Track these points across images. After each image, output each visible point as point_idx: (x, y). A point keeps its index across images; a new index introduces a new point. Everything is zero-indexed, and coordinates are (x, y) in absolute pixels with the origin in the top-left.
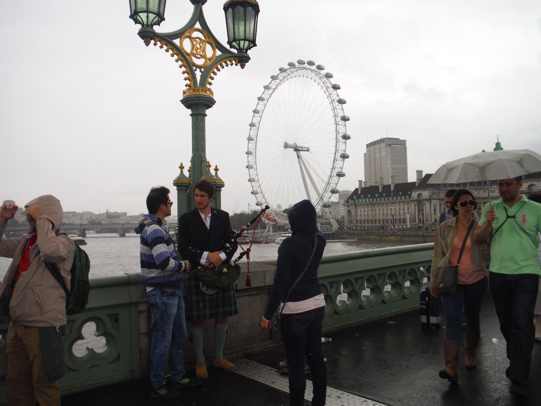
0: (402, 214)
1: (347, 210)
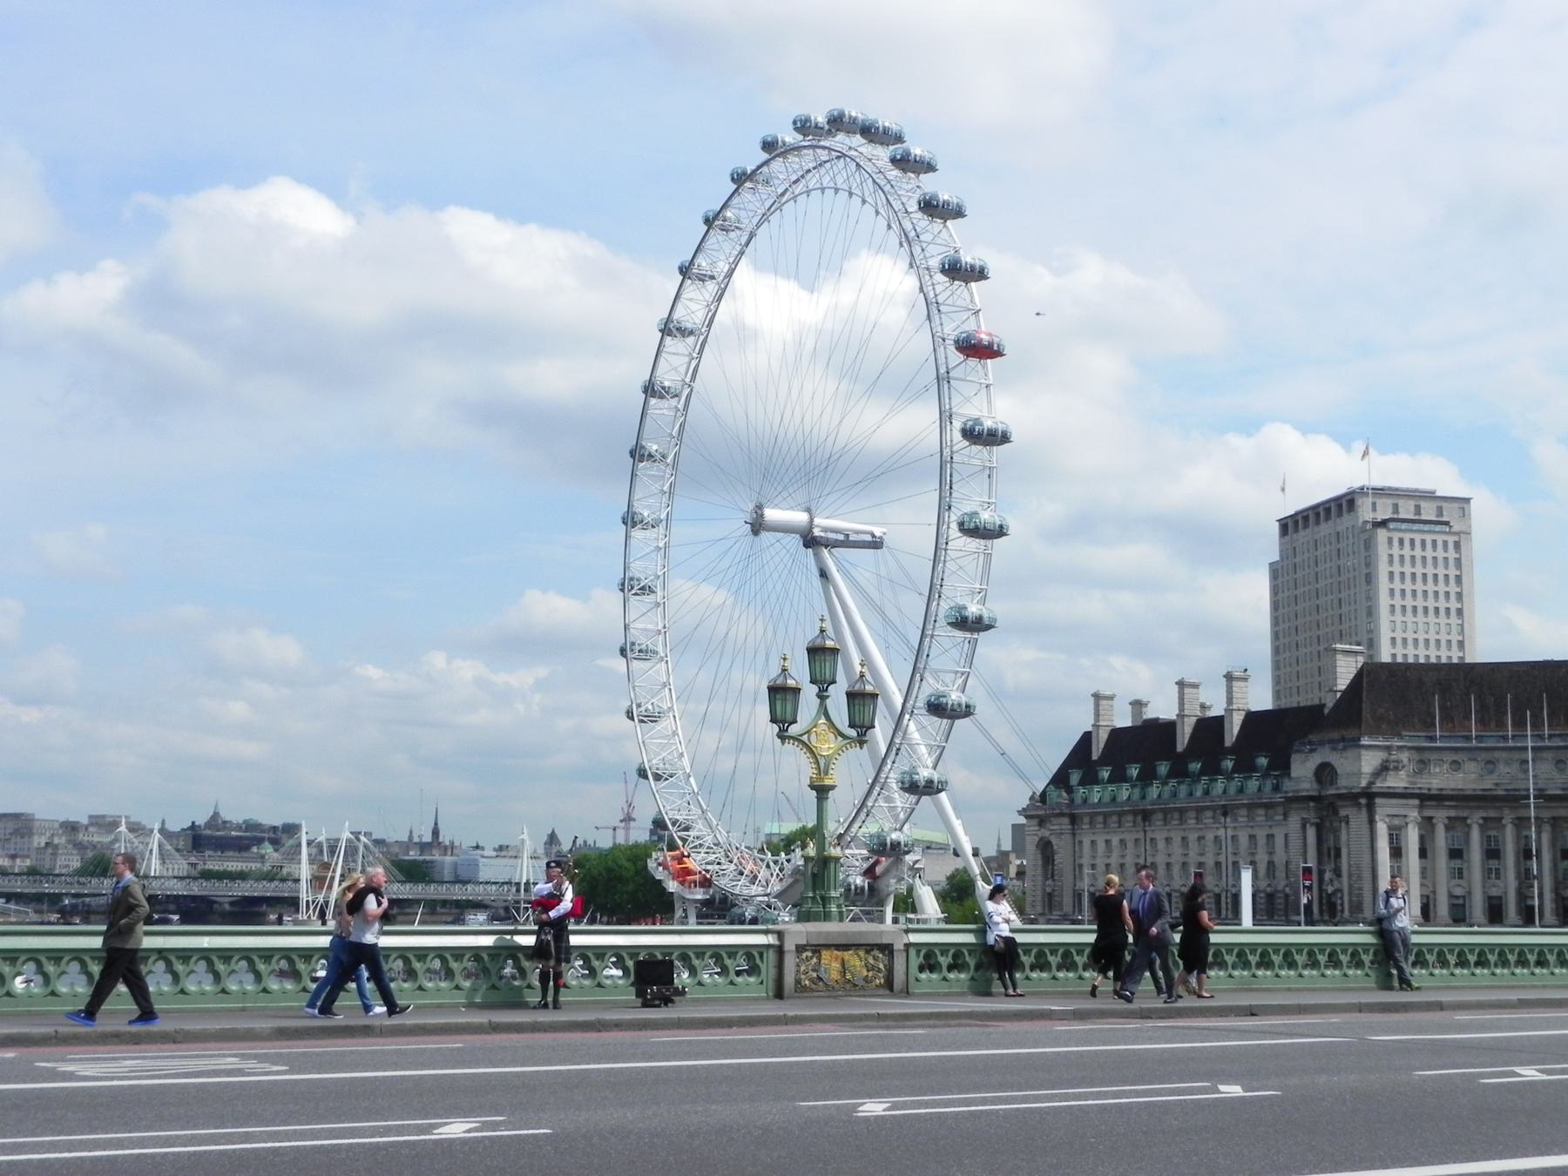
1: (1037, 839)
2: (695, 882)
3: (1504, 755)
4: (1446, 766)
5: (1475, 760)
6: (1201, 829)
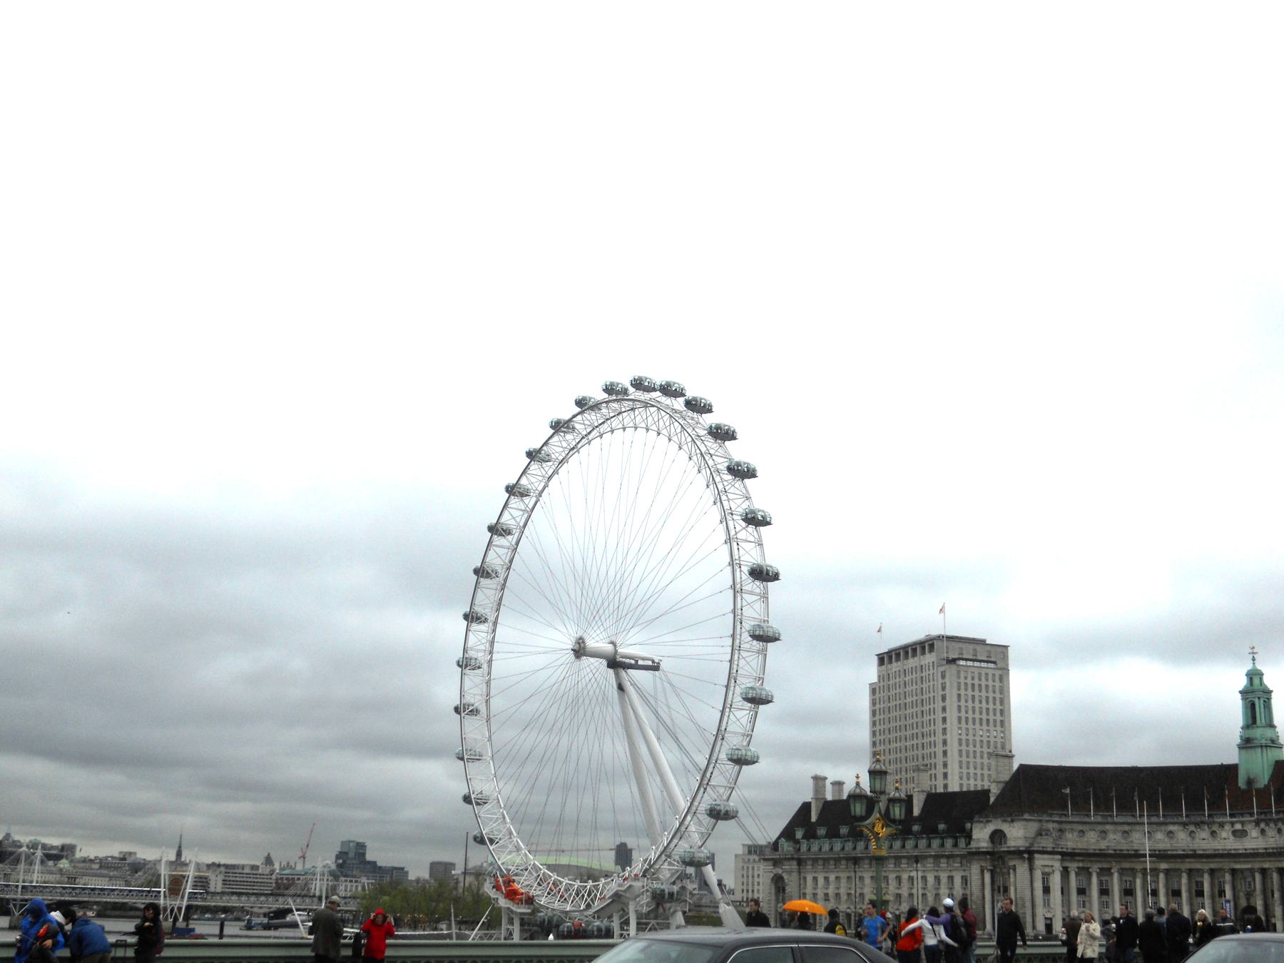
1: (772, 875)
2: (521, 900)
4: (1076, 834)
6: (898, 871)
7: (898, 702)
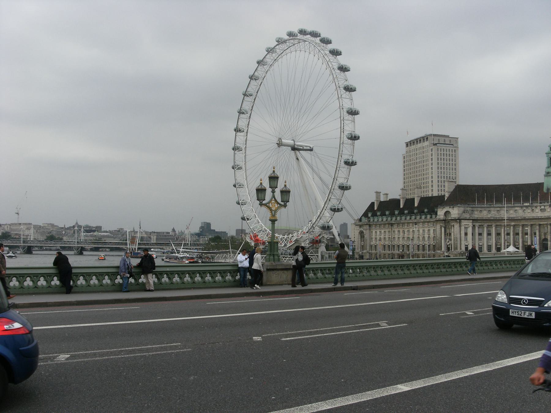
0: (426, 239)
1: (359, 231)
3: (493, 209)
5: (486, 210)
6: (408, 228)
7: (414, 162)
